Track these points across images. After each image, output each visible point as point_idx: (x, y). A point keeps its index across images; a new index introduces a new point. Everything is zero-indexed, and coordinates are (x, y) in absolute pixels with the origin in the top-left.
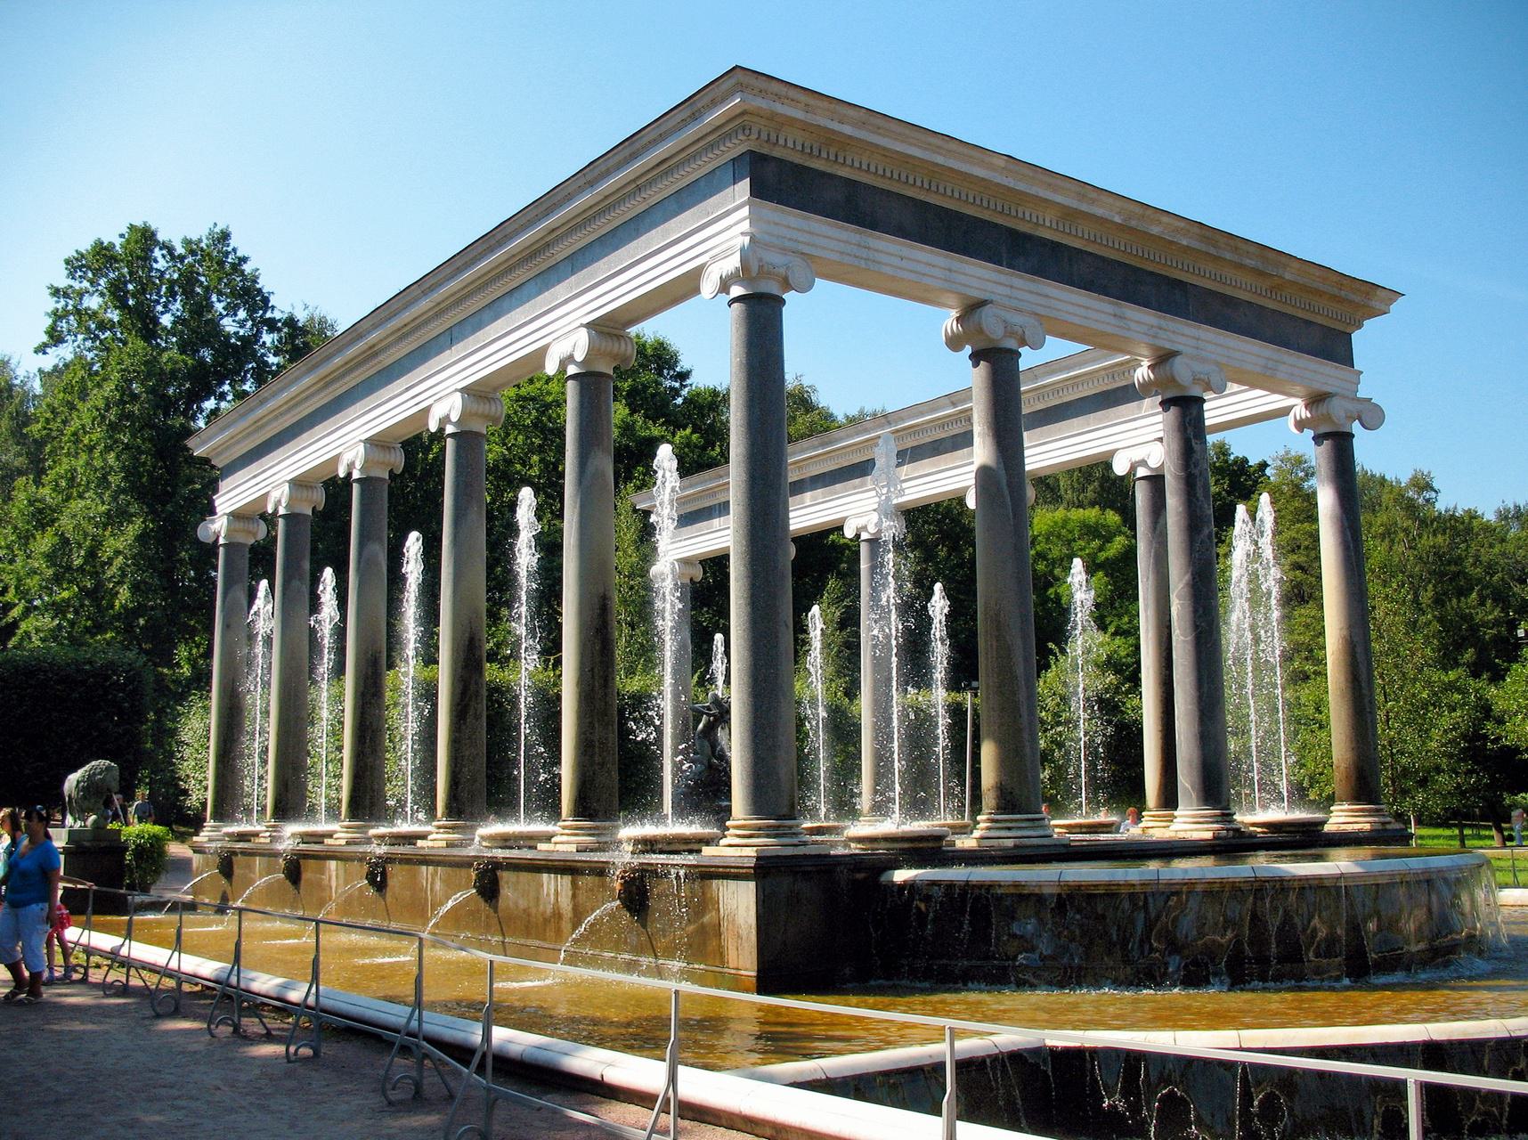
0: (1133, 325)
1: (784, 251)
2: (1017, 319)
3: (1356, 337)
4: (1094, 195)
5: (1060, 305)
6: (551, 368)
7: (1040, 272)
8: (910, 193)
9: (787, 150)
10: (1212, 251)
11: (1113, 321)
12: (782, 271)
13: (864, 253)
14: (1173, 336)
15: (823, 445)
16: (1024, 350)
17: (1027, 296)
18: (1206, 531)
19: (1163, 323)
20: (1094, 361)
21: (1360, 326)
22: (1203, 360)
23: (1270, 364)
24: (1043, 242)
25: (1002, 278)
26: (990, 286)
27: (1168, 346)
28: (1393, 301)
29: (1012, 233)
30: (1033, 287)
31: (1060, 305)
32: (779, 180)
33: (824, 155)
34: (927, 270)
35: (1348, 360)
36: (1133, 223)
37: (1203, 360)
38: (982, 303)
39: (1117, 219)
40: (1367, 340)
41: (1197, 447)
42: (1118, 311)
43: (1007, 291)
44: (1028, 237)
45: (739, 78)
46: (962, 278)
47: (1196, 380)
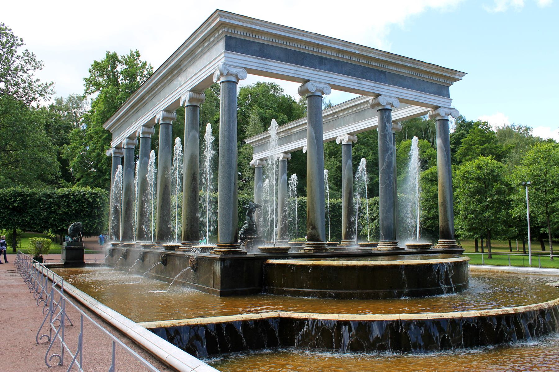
1: (236, 67)
2: (321, 86)
3: (451, 87)
4: (348, 44)
6: (181, 104)
7: (331, 70)
8: (283, 47)
9: (239, 34)
10: (394, 61)
12: (235, 73)
13: (265, 66)
15: (296, 123)
16: (324, 96)
18: (390, 152)
19: (376, 85)
20: (364, 98)
21: (452, 84)
22: (390, 97)
23: (417, 97)
24: (332, 60)
25: (316, 73)
26: (311, 75)
27: (378, 92)
28: (463, 76)
29: (320, 57)
30: (327, 75)
32: (234, 44)
33: (251, 36)
35: (448, 95)
36: (363, 53)
37: (390, 97)
38: (309, 81)
39: (357, 52)
40: (454, 89)
41: (387, 125)
42: (359, 82)
44: (326, 59)
45: (219, 12)
46: (301, 73)
47: (388, 103)
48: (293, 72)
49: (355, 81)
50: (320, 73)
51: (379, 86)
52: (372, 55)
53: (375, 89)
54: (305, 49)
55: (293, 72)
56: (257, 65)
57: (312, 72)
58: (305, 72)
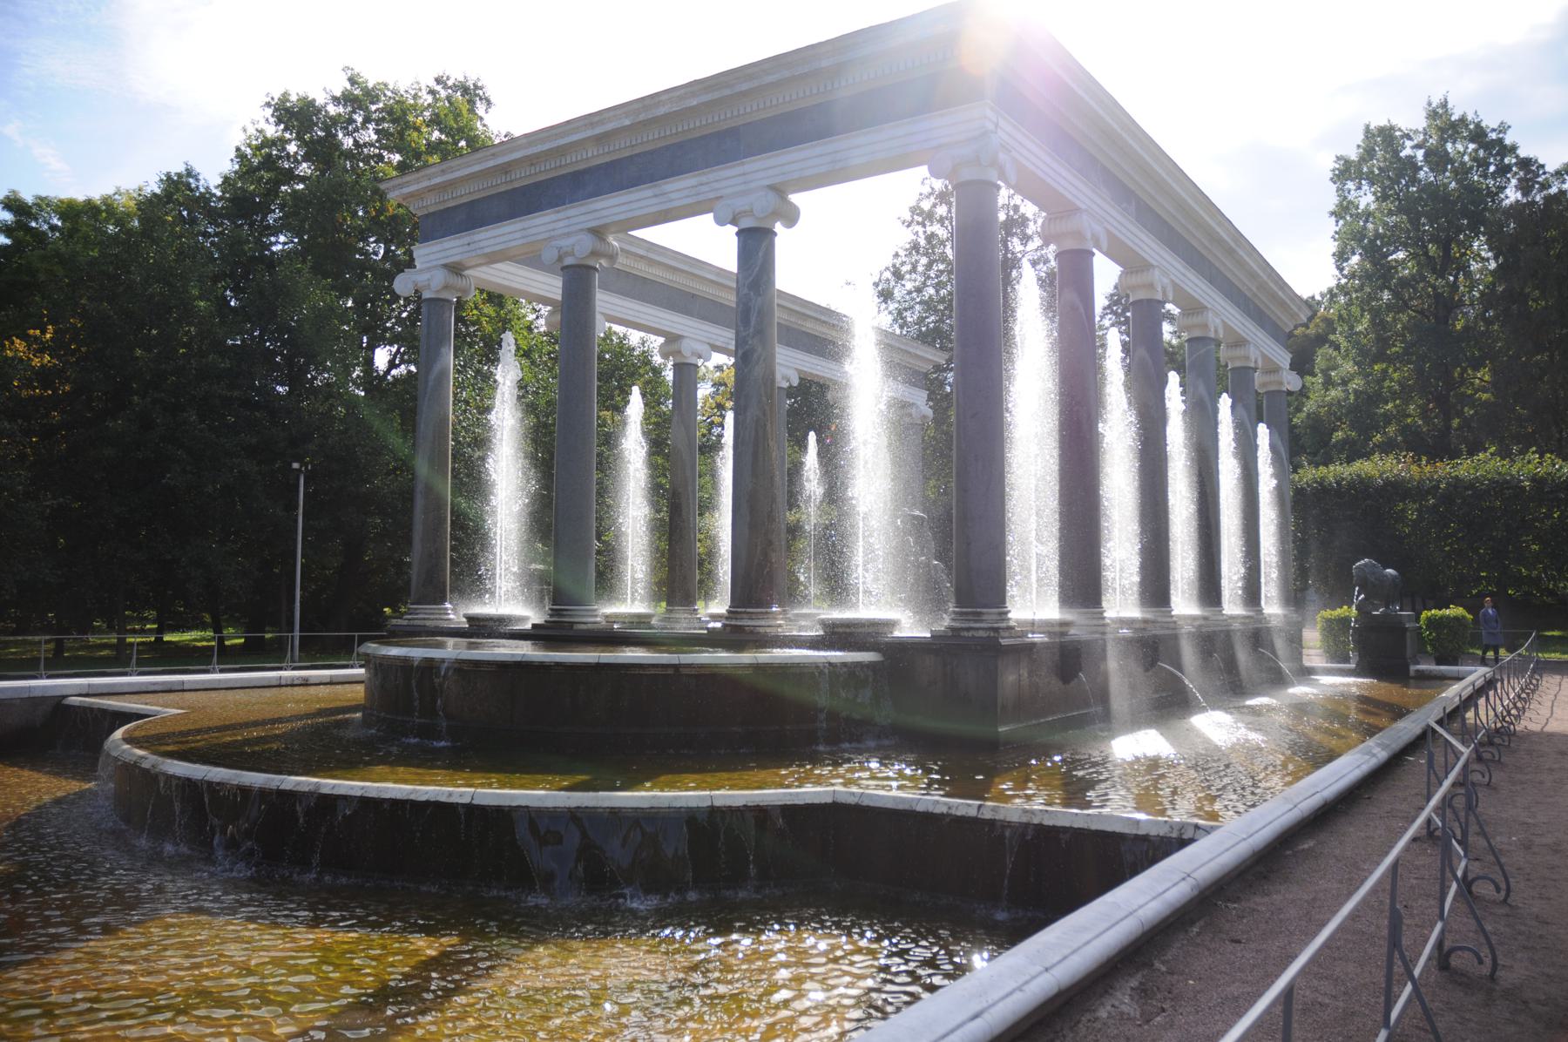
0: (673, 196)
5: (605, 213)
10: (727, 92)
11: (654, 201)
14: (716, 185)
17: (583, 218)
19: (704, 179)
24: (599, 167)
25: (560, 216)
26: (551, 227)
27: (711, 195)
31: (605, 213)
34: (511, 237)
36: (642, 117)
39: (627, 122)
42: (657, 191)
43: (566, 222)
48: (518, 235)
49: (649, 193)
50: (571, 212)
51: (712, 176)
52: (662, 111)
53: (704, 188)
54: (543, 172)
55: (518, 235)
56: (461, 250)
57: (554, 217)
58: (541, 224)
